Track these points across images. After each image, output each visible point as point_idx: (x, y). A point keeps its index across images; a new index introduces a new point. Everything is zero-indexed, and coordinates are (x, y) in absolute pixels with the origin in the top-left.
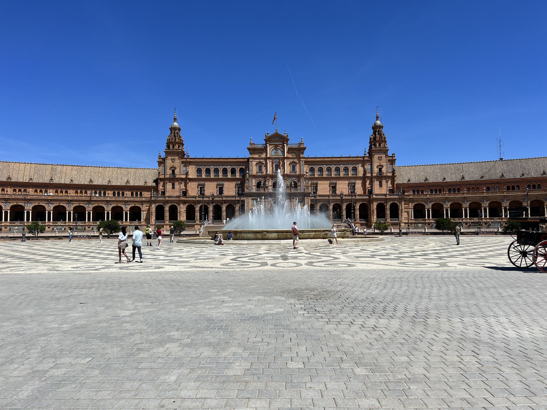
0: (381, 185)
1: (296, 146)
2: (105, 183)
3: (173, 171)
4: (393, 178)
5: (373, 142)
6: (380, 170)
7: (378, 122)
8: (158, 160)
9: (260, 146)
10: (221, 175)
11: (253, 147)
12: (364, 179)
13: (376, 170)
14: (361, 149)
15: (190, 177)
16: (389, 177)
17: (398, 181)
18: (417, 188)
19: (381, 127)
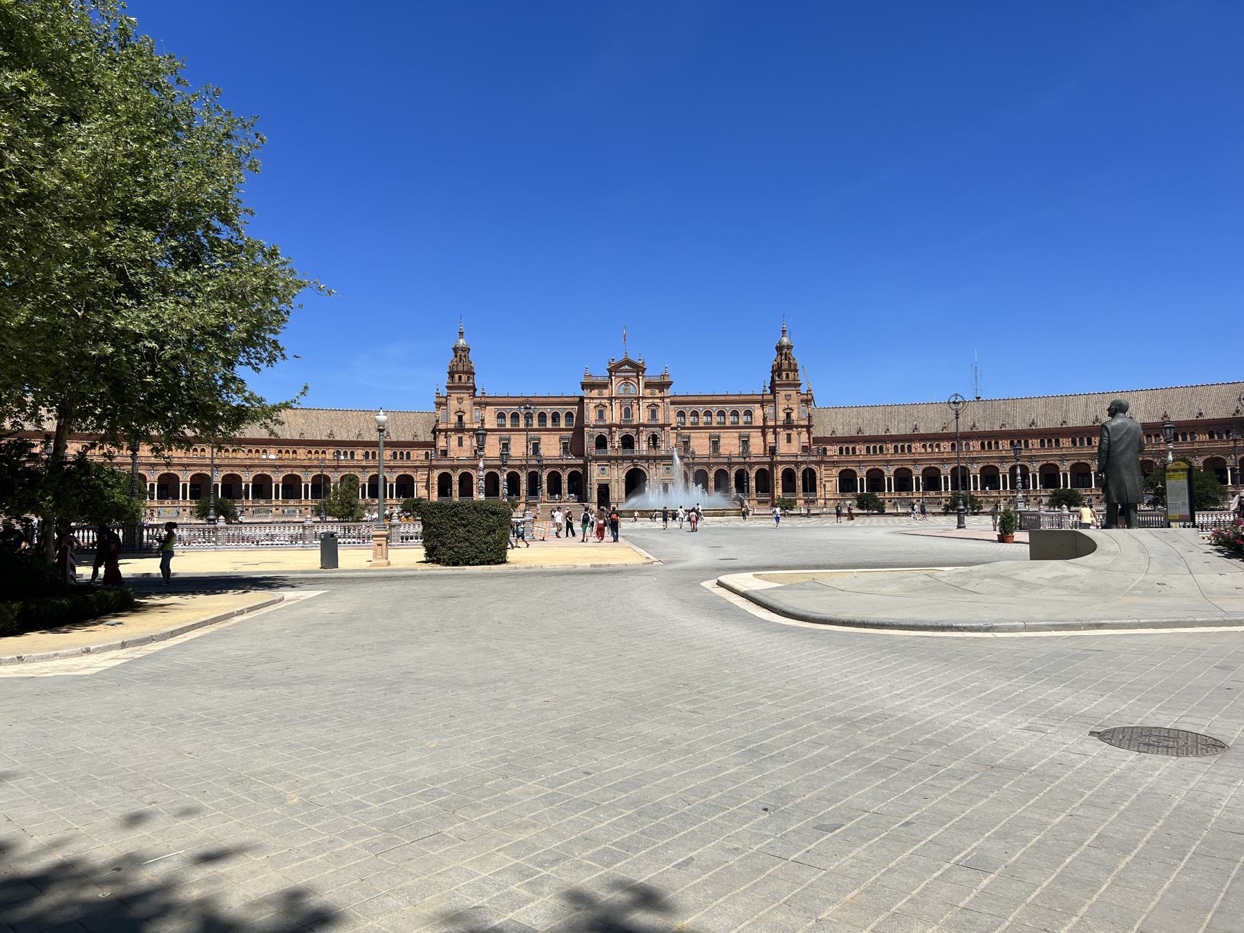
0: (789, 440)
1: (657, 380)
2: (352, 437)
3: (460, 418)
4: (808, 427)
5: (777, 370)
6: (788, 415)
7: (785, 340)
8: (436, 400)
9: (600, 380)
10: (535, 424)
11: (591, 380)
12: (764, 429)
13: (782, 415)
14: (758, 383)
15: (487, 426)
16: (802, 427)
17: (817, 433)
18: (846, 442)
19: (789, 347)
